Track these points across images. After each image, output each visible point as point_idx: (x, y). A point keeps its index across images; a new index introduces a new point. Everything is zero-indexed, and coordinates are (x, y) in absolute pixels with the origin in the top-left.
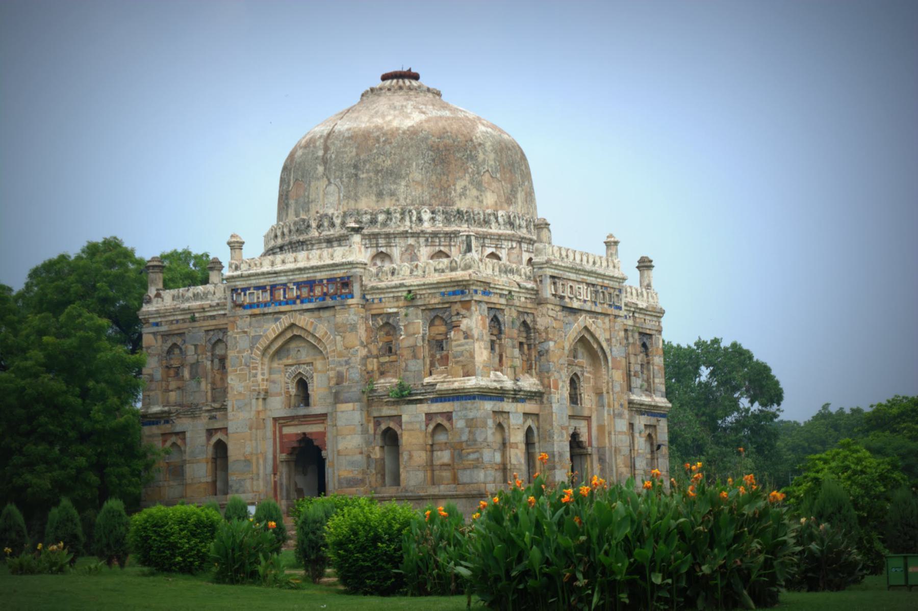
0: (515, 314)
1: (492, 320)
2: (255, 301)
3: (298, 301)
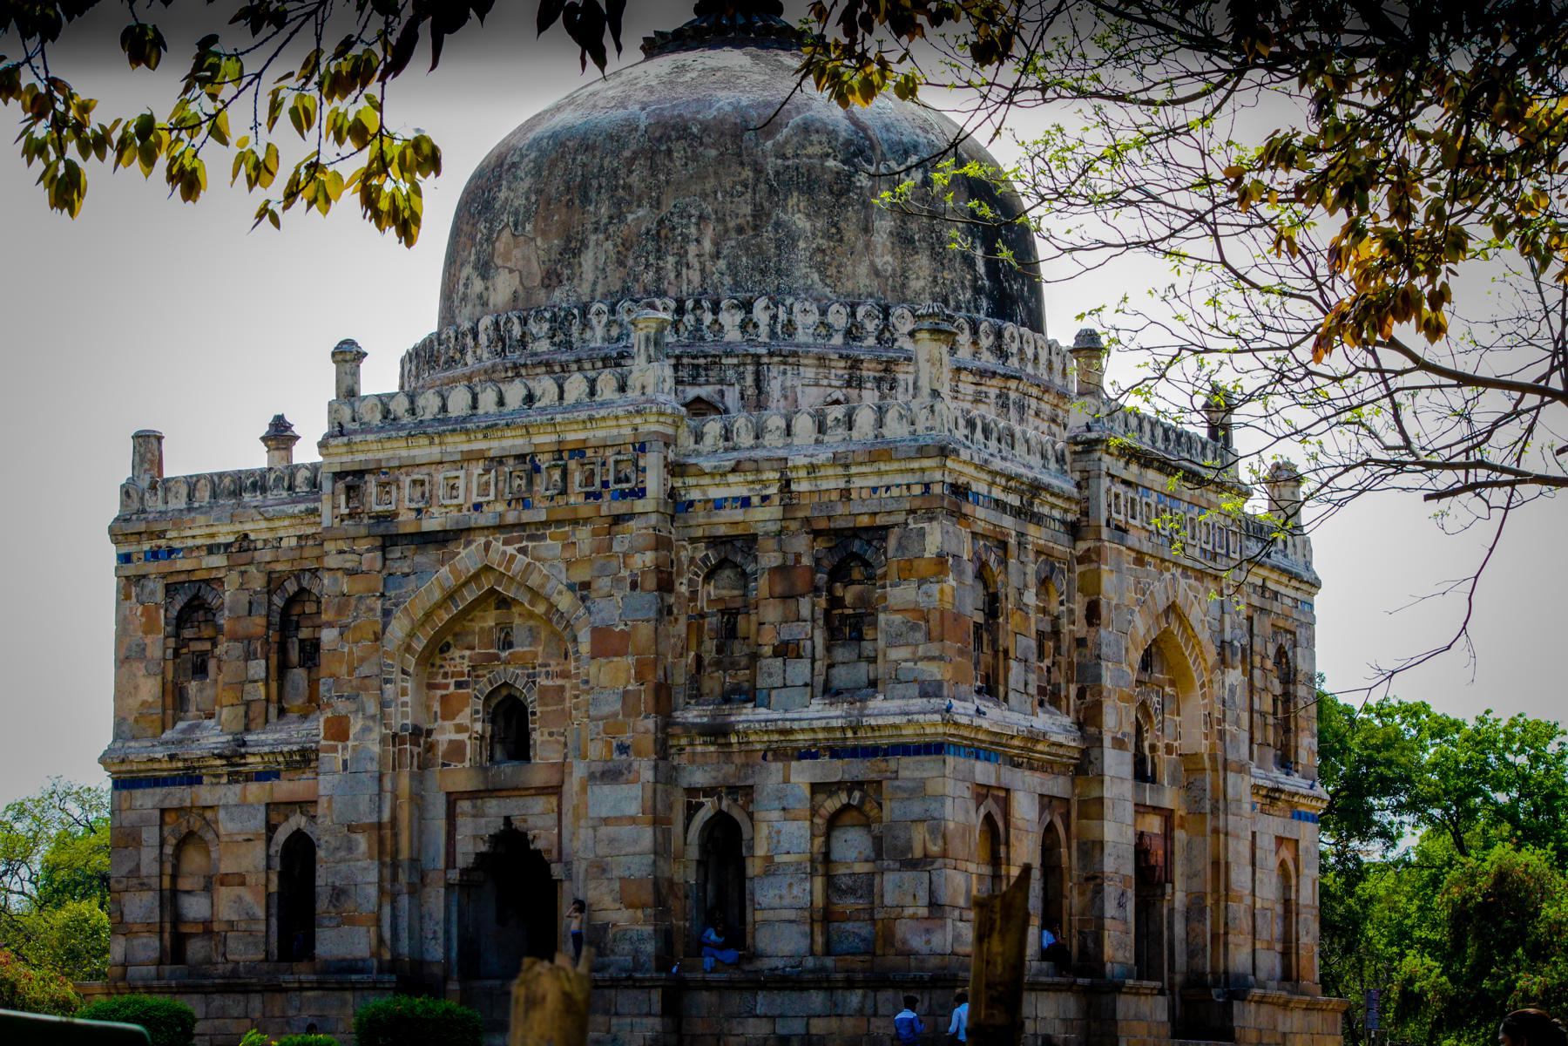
0: (258, 582)
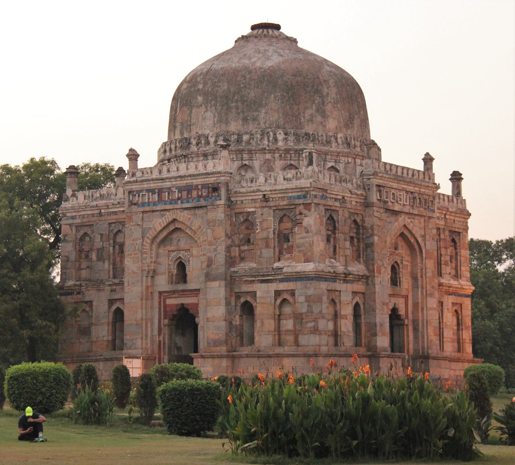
0: (347, 215)
1: (328, 219)
3: (179, 202)
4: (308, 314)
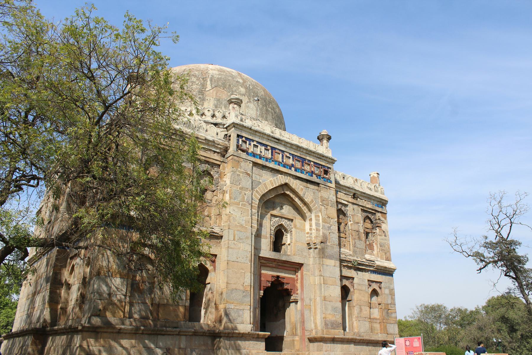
2: (259, 153)
3: (293, 169)
4: (392, 306)
